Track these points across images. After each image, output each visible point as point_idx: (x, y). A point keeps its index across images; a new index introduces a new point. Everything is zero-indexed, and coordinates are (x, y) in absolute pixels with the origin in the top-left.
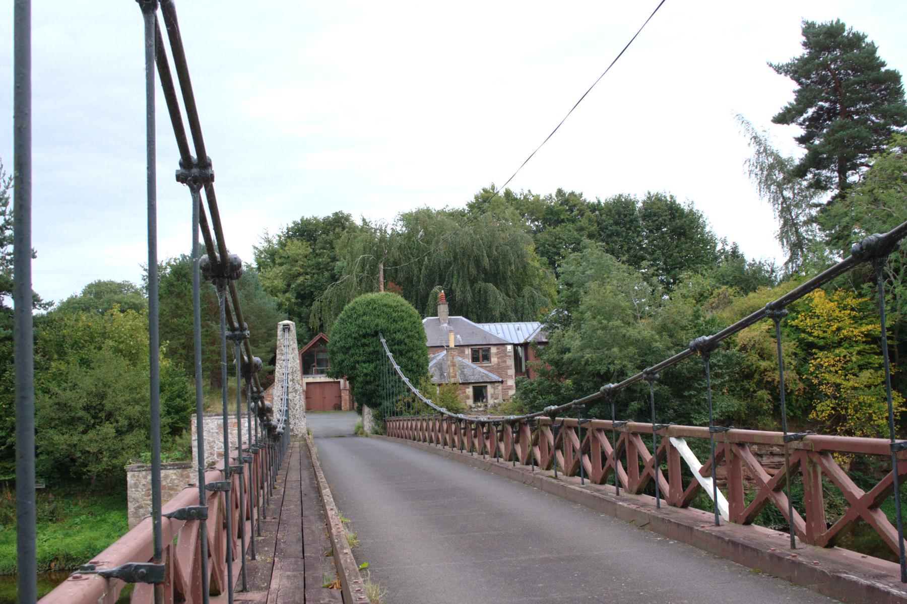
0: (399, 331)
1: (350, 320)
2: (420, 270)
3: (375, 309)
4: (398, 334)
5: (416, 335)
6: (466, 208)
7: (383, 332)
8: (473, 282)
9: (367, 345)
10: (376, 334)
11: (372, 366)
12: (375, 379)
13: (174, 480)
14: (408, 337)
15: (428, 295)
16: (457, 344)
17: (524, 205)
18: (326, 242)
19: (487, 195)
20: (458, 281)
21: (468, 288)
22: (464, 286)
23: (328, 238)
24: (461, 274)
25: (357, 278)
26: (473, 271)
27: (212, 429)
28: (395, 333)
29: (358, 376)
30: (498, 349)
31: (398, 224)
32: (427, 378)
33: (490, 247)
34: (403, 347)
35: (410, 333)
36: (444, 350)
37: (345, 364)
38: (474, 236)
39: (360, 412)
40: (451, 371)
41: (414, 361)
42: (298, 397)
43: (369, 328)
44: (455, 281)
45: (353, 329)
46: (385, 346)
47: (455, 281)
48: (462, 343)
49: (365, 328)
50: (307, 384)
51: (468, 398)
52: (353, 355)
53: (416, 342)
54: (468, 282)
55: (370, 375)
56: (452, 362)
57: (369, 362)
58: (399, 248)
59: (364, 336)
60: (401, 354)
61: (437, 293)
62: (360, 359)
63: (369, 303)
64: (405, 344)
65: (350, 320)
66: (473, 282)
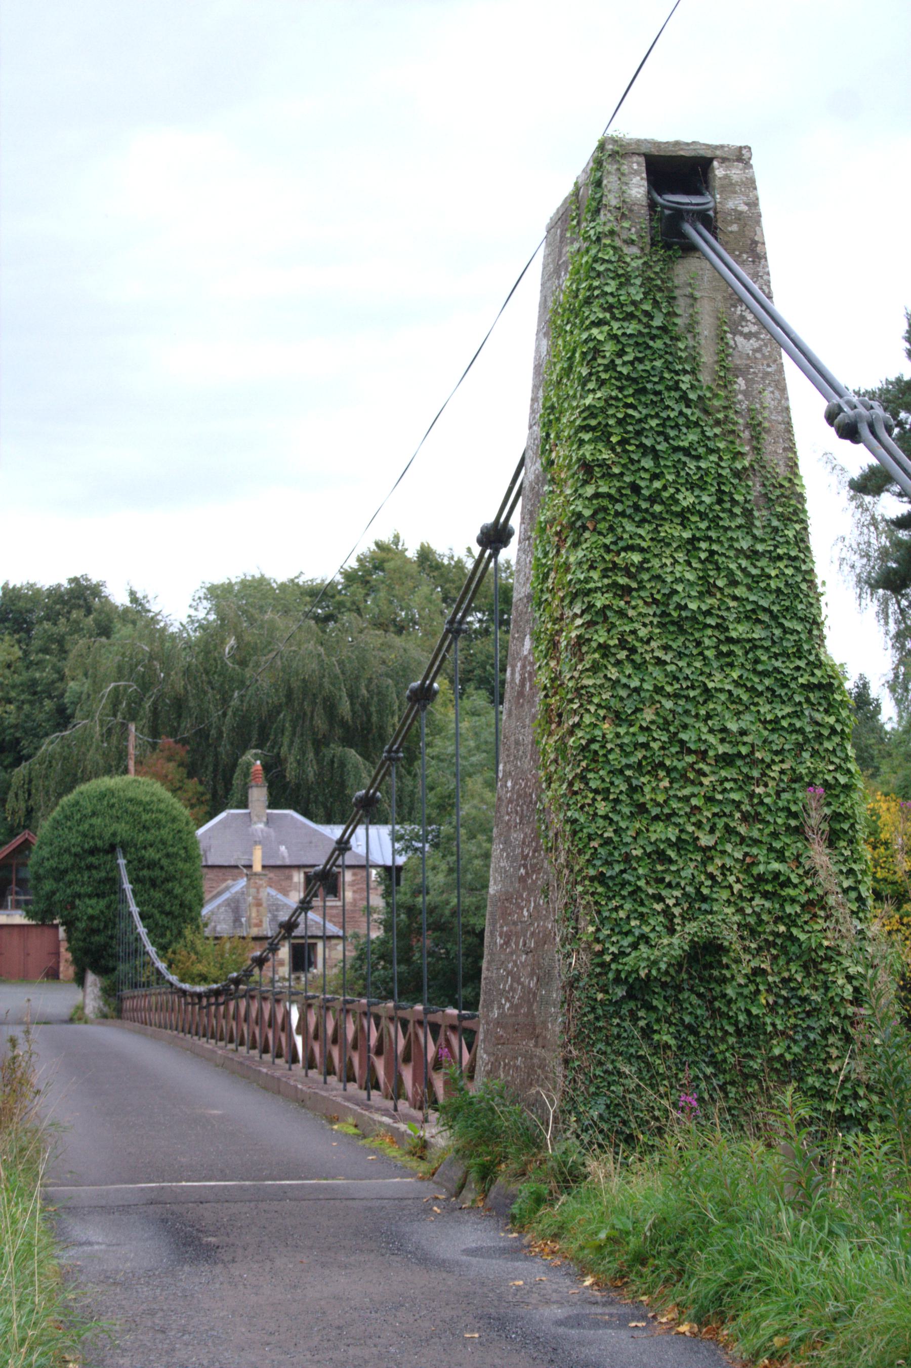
0: (151, 846)
1: (69, 824)
2: (225, 714)
3: (113, 806)
4: (150, 850)
5: (182, 852)
6: (339, 578)
7: (125, 846)
8: (319, 744)
9: (96, 868)
10: (112, 849)
11: (103, 903)
12: (106, 927)
14: (168, 855)
15: (235, 765)
16: (272, 862)
17: (453, 582)
18: (51, 639)
19: (384, 555)
21: (311, 755)
23: (55, 630)
25: (102, 726)
26: (320, 723)
28: (145, 848)
29: (78, 919)
30: (354, 874)
31: (200, 607)
32: (198, 927)
33: (357, 678)
34: (157, 872)
35: (171, 850)
36: (241, 875)
37: (57, 897)
38: (326, 659)
39: (80, 980)
40: (254, 915)
41: (176, 897)
43: (101, 838)
44: (286, 741)
45: (74, 838)
46: (124, 872)
47: (286, 741)
48: (288, 862)
49: (93, 838)
51: (282, 964)
52: (71, 883)
53: (181, 865)
54: (310, 745)
55: (98, 919)
56: (255, 898)
57: (98, 896)
58: (187, 672)
59: (92, 852)
60: (154, 884)
61: (249, 765)
62: (82, 891)
63: (102, 796)
64: (162, 868)
65: (69, 824)
66: (319, 744)
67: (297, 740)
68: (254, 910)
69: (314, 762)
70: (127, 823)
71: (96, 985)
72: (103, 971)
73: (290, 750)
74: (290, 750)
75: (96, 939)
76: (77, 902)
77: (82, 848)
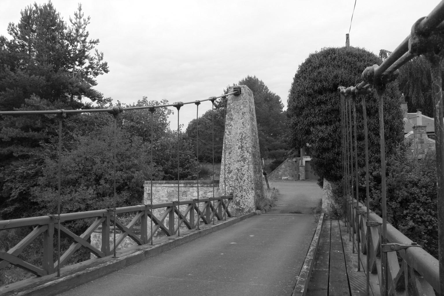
3: (334, 59)
11: (330, 128)
12: (333, 146)
13: (128, 244)
20: (413, 90)
22: (418, 93)
24: (415, 85)
27: (163, 196)
42: (246, 166)
43: (326, 80)
44: (410, 90)
50: (306, 162)
52: (307, 116)
57: (326, 123)
62: (314, 120)
67: (415, 89)
68: (420, 145)
69: (423, 97)
70: (345, 69)
71: (329, 188)
72: (335, 179)
73: (413, 93)
74: (413, 93)
75: (326, 155)
76: (312, 129)
77: (313, 89)
